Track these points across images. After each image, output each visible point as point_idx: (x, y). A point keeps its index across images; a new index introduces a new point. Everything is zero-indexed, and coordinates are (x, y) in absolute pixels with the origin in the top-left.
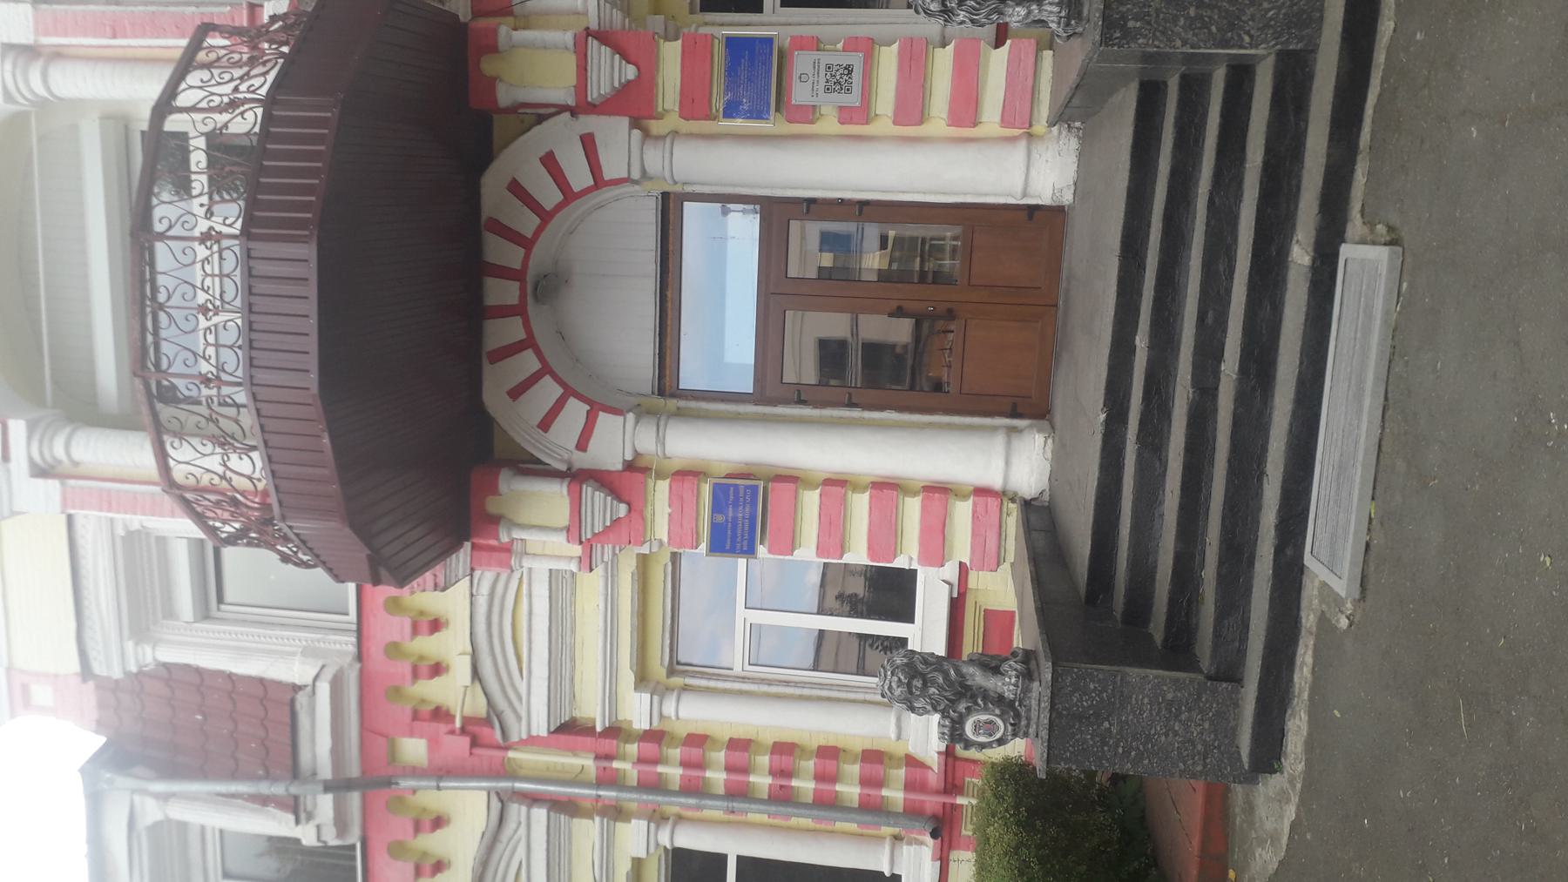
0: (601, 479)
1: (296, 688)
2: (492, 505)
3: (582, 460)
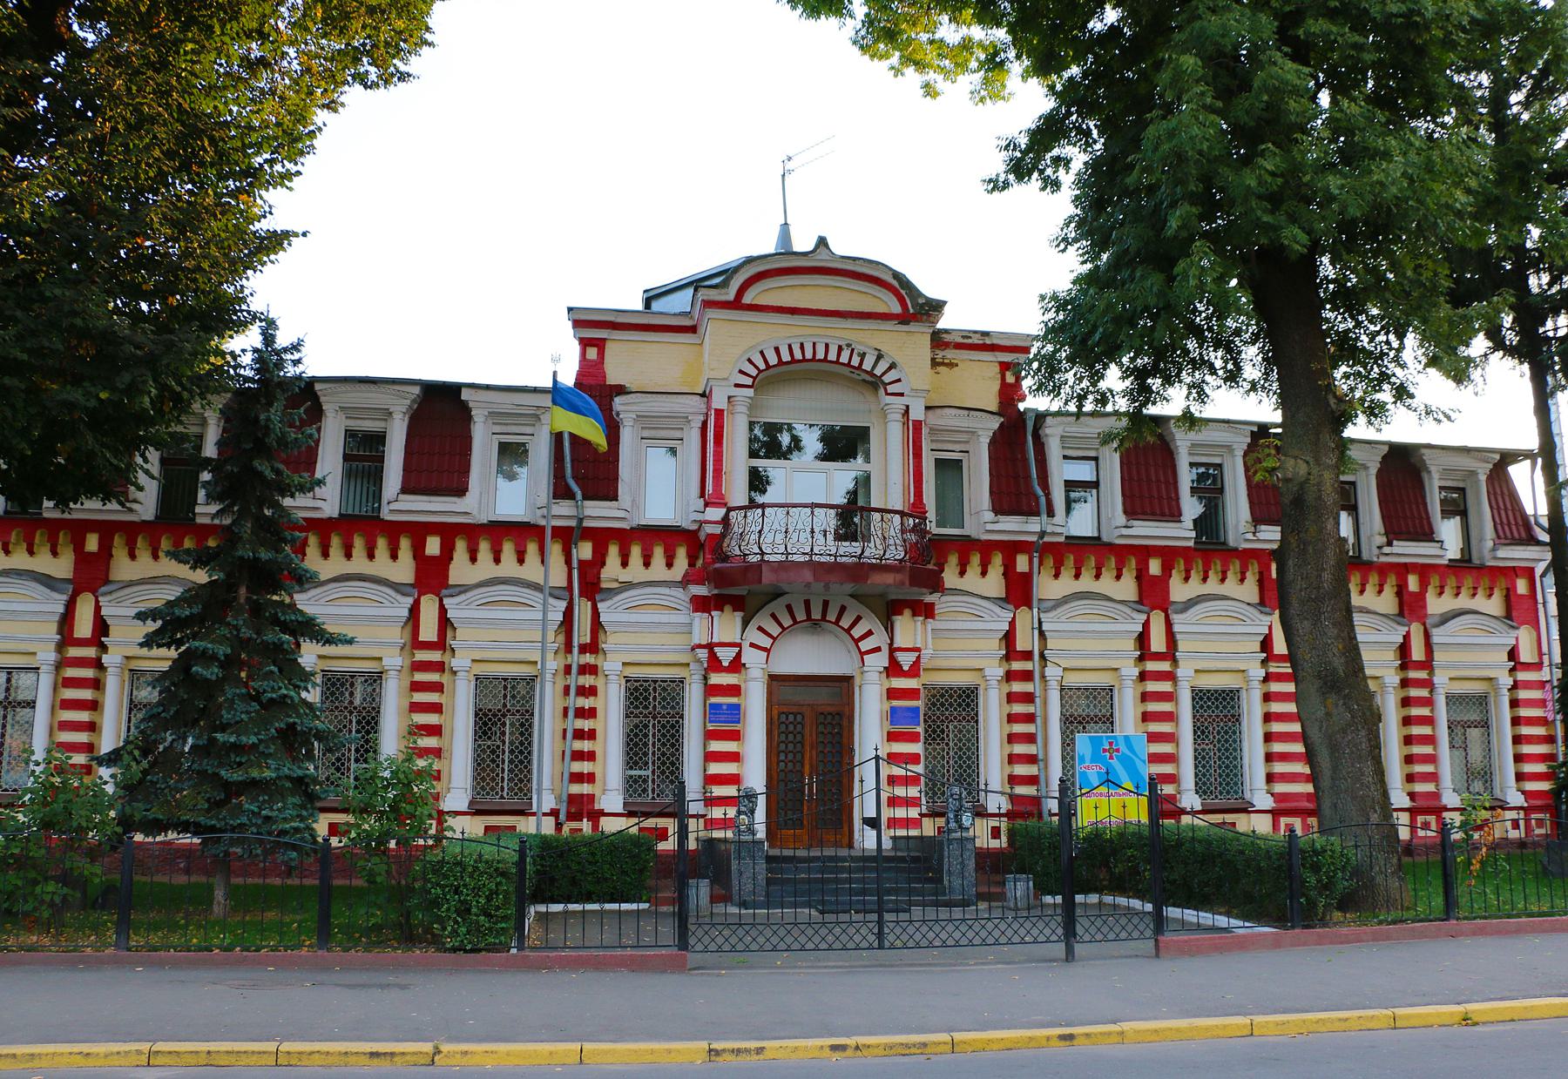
0: (739, 655)
2: (728, 608)
3: (745, 645)
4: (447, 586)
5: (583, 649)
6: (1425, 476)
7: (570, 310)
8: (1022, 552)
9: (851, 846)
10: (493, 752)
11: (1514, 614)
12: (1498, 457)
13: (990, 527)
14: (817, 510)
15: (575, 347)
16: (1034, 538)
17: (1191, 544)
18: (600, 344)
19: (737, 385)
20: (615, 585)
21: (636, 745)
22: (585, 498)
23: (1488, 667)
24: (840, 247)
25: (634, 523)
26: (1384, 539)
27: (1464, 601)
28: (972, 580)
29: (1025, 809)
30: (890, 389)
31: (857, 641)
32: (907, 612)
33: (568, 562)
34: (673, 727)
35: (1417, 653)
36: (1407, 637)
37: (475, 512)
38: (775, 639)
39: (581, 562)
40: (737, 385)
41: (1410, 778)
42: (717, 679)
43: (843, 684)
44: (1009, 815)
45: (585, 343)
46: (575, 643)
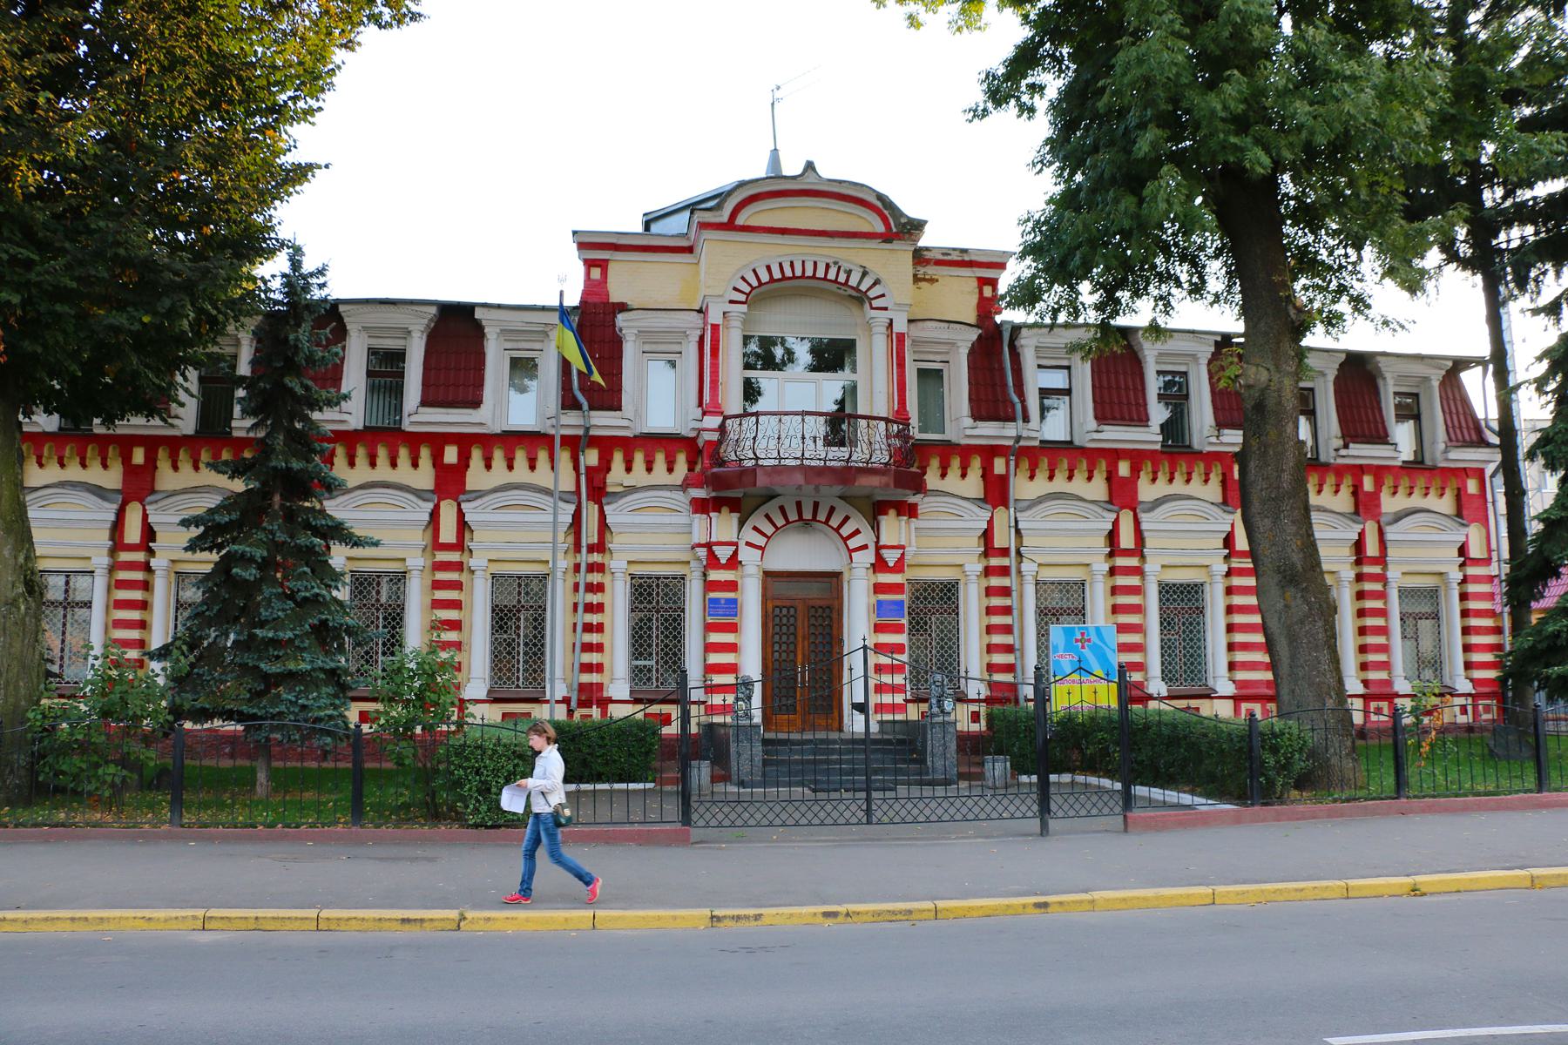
0: (736, 553)
1: (619, 408)
2: (725, 510)
4: (464, 492)
5: (591, 549)
6: (1380, 383)
7: (575, 233)
8: (1000, 455)
9: (840, 729)
10: (509, 645)
11: (1465, 512)
12: (1450, 364)
13: (969, 432)
14: (807, 418)
15: (580, 268)
16: (1011, 443)
17: (1158, 447)
18: (603, 265)
19: (731, 302)
20: (620, 489)
21: (641, 637)
22: (591, 408)
23: (1440, 562)
24: (827, 170)
25: (637, 432)
26: (1341, 442)
27: (1417, 501)
28: (953, 482)
29: (1002, 695)
30: (875, 303)
31: (845, 540)
32: (892, 512)
33: (576, 468)
34: (675, 620)
35: (1372, 549)
36: (1362, 534)
37: (489, 423)
38: (769, 538)
39: (588, 469)
40: (731, 302)
41: (1364, 667)
42: (715, 575)
43: (833, 579)
44: (988, 701)
45: (589, 264)
46: (584, 543)
